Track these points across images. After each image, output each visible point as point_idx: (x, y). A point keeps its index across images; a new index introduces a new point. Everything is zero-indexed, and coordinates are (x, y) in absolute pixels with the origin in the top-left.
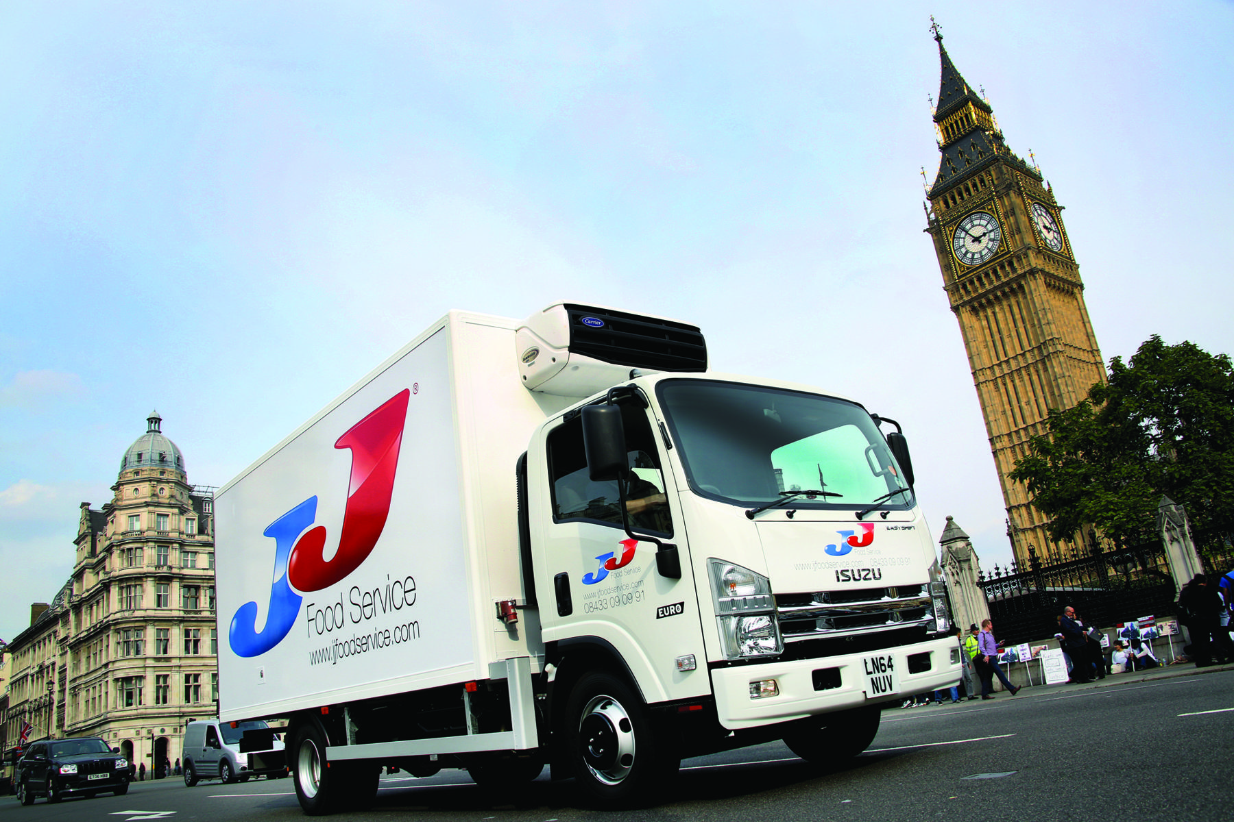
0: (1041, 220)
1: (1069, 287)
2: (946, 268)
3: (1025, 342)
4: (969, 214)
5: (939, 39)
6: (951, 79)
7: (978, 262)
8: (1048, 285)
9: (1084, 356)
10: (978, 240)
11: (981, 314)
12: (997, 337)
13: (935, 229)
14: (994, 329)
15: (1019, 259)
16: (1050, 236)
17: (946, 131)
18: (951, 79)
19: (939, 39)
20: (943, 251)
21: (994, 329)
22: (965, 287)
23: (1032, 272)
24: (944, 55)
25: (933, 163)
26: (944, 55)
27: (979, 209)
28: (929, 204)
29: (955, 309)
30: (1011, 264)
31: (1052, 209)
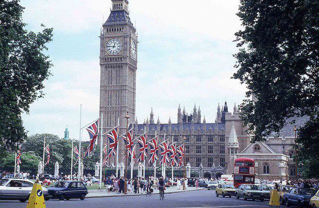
1: (133, 69)
2: (102, 51)
3: (118, 83)
4: (114, 38)
7: (112, 54)
9: (132, 90)
10: (115, 47)
11: (108, 69)
13: (102, 38)
14: (110, 75)
16: (133, 52)
20: (103, 46)
21: (110, 75)
22: (106, 59)
23: (126, 64)
25: (107, 14)
28: (102, 28)
29: (101, 65)
30: (121, 59)
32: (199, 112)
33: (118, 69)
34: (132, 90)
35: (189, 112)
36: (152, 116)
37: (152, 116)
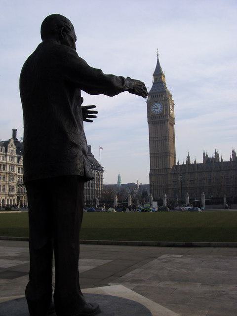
0: (171, 108)
5: (158, 55)
6: (158, 68)
8: (170, 124)
10: (158, 108)
12: (156, 131)
15: (166, 116)
16: (172, 111)
17: (155, 79)
18: (158, 68)
19: (158, 55)
24: (158, 59)
26: (158, 59)
27: (160, 102)
30: (164, 116)
31: (173, 105)
32: (218, 155)
33: (162, 124)
34: (172, 140)
35: (211, 155)
36: (188, 157)
37: (188, 157)
